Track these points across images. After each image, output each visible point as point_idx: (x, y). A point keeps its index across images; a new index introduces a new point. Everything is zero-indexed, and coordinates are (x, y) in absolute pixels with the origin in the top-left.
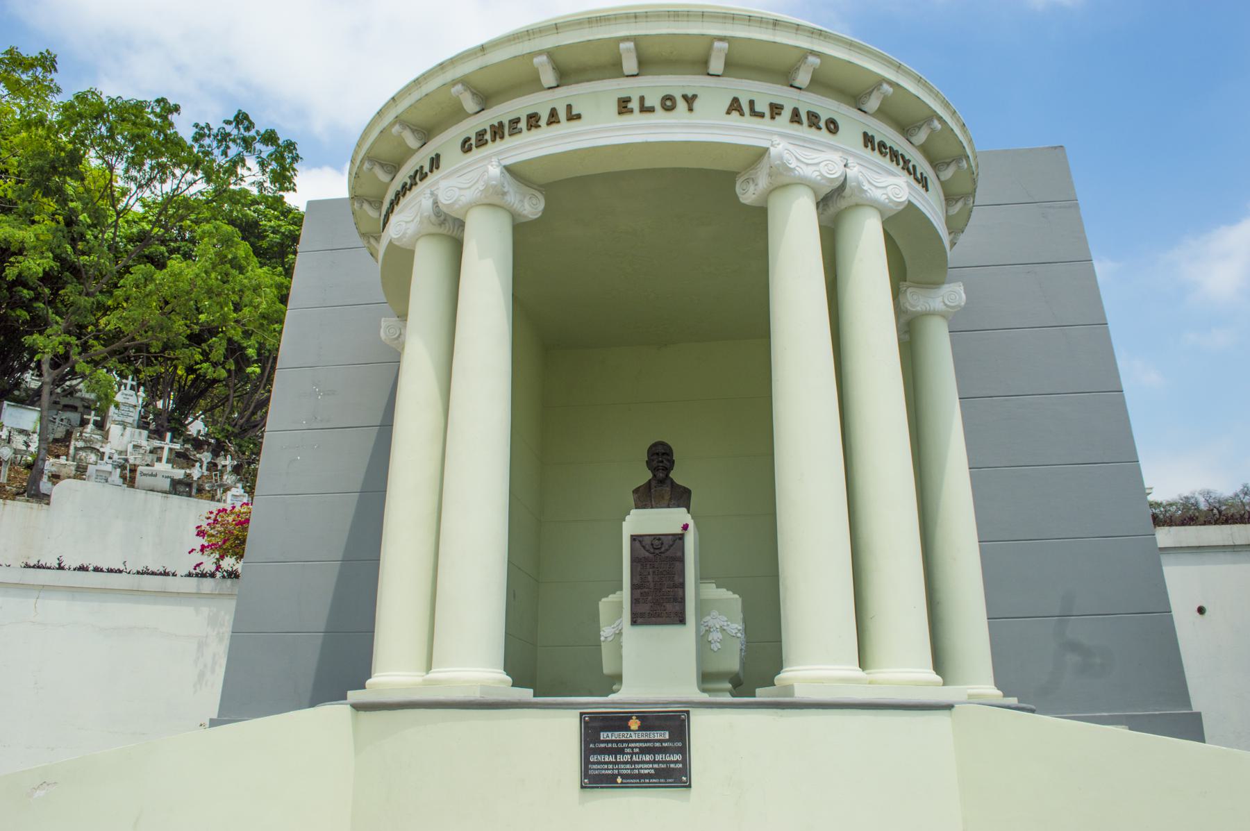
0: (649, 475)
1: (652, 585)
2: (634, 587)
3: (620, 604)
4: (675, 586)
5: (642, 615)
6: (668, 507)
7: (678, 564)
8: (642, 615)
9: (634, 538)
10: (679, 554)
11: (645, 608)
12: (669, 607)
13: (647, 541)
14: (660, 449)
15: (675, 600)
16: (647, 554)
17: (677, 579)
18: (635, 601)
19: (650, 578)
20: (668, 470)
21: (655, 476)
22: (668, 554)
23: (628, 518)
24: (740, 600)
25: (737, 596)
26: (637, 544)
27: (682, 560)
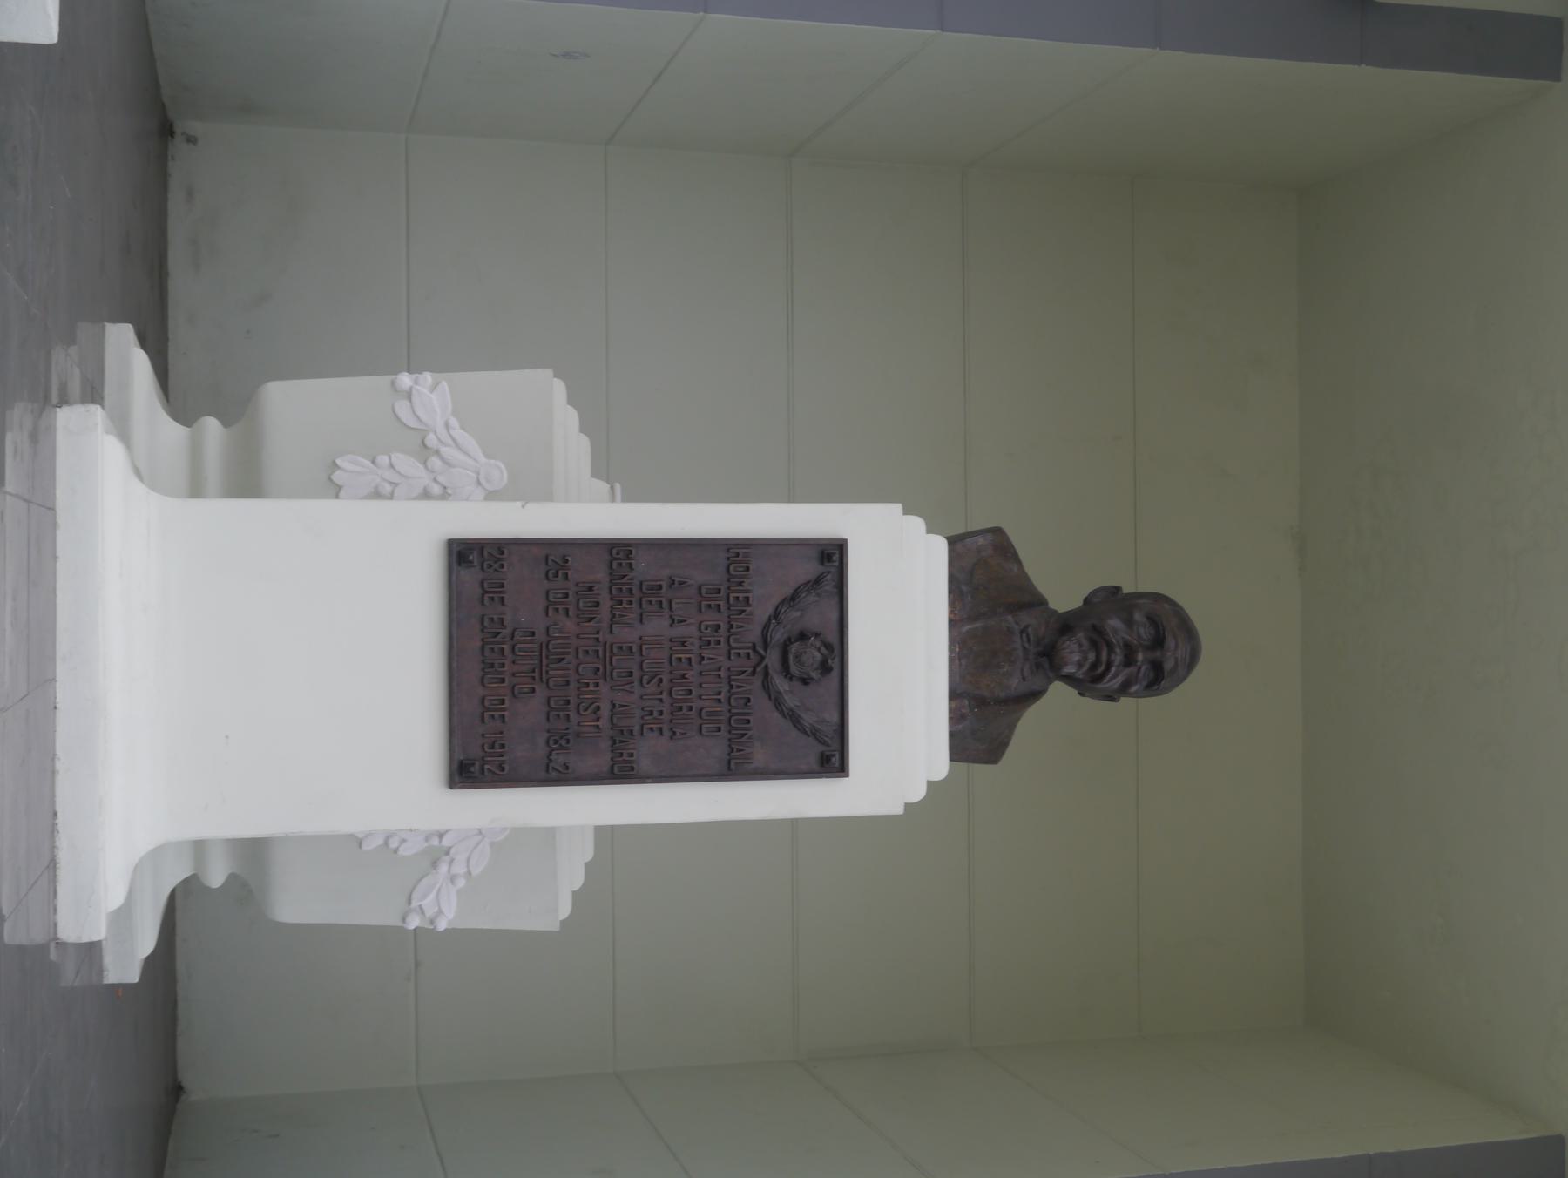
0: (1064, 597)
1: (627, 634)
2: (619, 552)
3: (531, 485)
4: (620, 740)
5: (493, 591)
6: (953, 695)
7: (716, 748)
8: (493, 591)
9: (832, 555)
10: (759, 756)
11: (525, 607)
12: (529, 713)
13: (816, 615)
14: (1172, 655)
15: (559, 740)
16: (761, 611)
17: (646, 749)
18: (554, 556)
19: (657, 626)
20: (1089, 682)
21: (1066, 625)
22: (761, 704)
23: (917, 523)
24: (555, 927)
25: (565, 910)
26: (808, 569)
27: (734, 768)
